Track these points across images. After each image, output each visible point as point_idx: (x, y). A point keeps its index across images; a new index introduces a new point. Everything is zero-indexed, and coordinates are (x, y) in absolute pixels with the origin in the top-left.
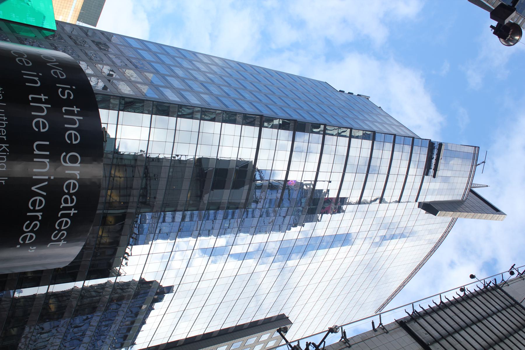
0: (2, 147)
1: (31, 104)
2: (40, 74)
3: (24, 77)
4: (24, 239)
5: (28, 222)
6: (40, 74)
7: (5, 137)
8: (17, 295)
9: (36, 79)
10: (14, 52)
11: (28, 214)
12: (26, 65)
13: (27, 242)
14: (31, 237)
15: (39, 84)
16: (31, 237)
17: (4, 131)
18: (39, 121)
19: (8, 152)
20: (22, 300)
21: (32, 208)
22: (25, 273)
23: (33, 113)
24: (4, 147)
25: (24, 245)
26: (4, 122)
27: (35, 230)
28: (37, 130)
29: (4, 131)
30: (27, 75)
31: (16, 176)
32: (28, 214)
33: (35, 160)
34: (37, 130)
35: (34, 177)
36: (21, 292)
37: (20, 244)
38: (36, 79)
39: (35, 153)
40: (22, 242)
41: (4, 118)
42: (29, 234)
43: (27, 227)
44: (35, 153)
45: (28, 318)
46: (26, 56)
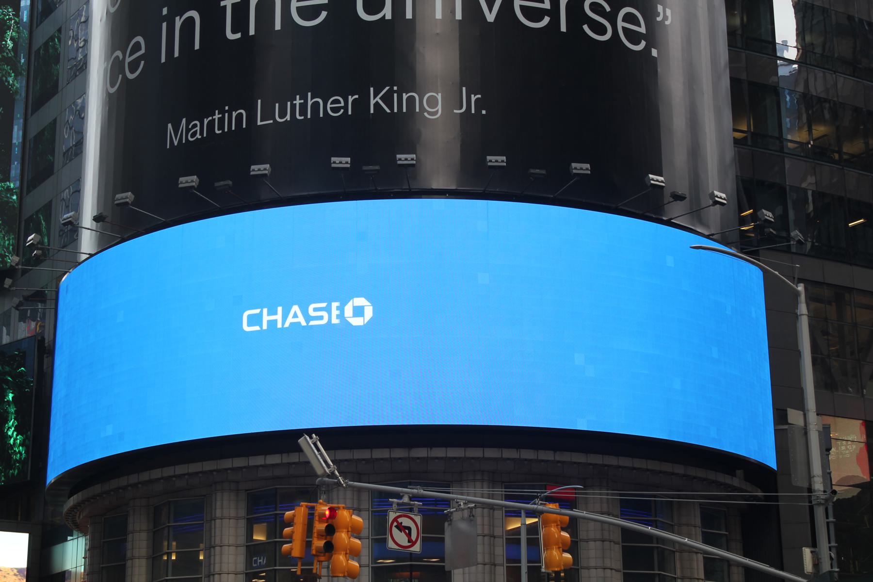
0: (377, 104)
1: (252, 32)
2: (165, 11)
3: (176, 54)
4: (634, 37)
5: (586, 27)
6: (165, 11)
7: (350, 99)
8: (792, 54)
9: (178, 22)
10: (112, 86)
11: (563, 28)
12: (143, 51)
13: (642, 30)
14: (629, 18)
15: (194, 14)
16: (629, 18)
17: (333, 102)
18: (298, 9)
19: (392, 88)
20: (808, 39)
21: (547, 20)
22: (731, 33)
23: (278, 27)
24: (378, 99)
25: (652, 37)
26: (310, 103)
27: (608, 9)
28: (324, 14)
29: (333, 102)
30: (170, 46)
31: (457, 66)
32: (563, 28)
33: (409, 15)
34: (324, 14)
35: (459, 16)
36: (785, 45)
37: (647, 49)
38: (178, 22)
39: (389, 17)
40: (643, 43)
41: (298, 102)
42: (620, 24)
43: (602, 30)
44: (389, 17)
45: (861, 21)
46: (119, 53)
